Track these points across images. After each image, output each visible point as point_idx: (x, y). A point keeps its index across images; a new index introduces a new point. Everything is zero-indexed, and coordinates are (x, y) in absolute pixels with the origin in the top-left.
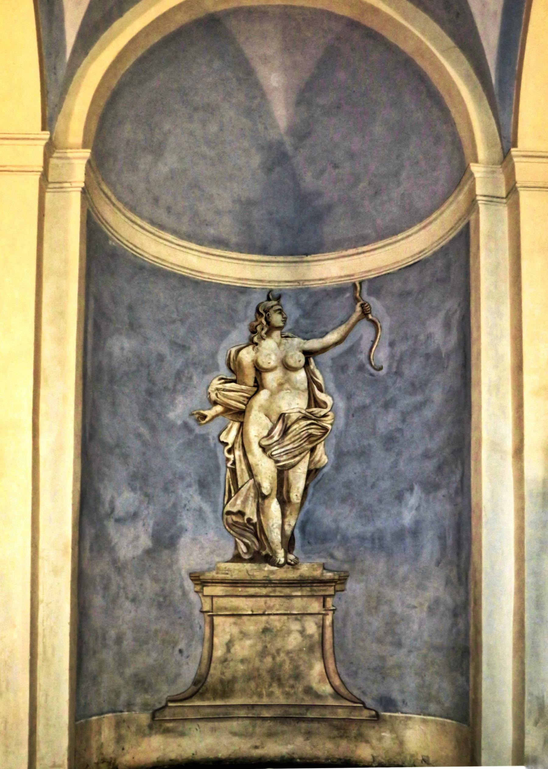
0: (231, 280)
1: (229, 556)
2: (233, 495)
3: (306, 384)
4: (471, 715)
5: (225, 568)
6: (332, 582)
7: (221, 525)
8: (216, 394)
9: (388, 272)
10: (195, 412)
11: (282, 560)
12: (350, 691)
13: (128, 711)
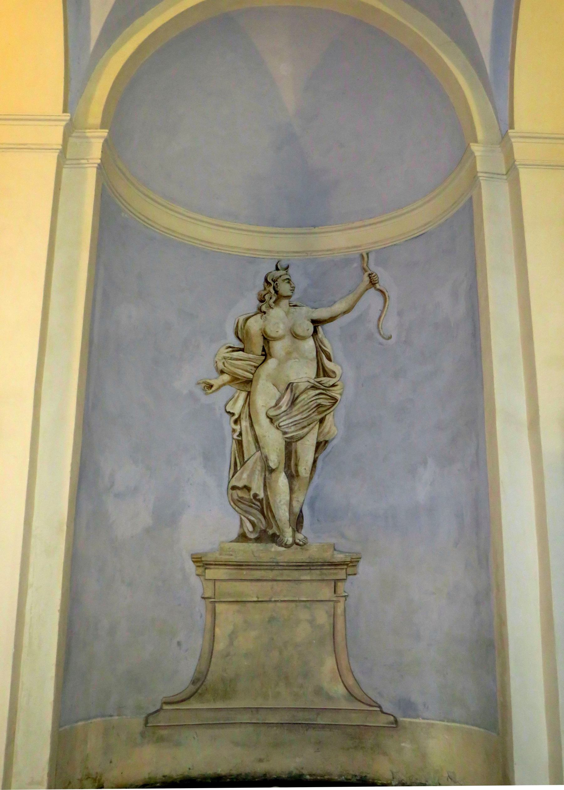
0: (239, 251)
1: (234, 534)
2: (238, 468)
3: (315, 353)
4: (500, 721)
5: (229, 548)
6: (344, 565)
7: (225, 501)
8: (224, 363)
9: (395, 243)
10: (201, 382)
11: (290, 540)
12: (365, 691)
13: (118, 715)
